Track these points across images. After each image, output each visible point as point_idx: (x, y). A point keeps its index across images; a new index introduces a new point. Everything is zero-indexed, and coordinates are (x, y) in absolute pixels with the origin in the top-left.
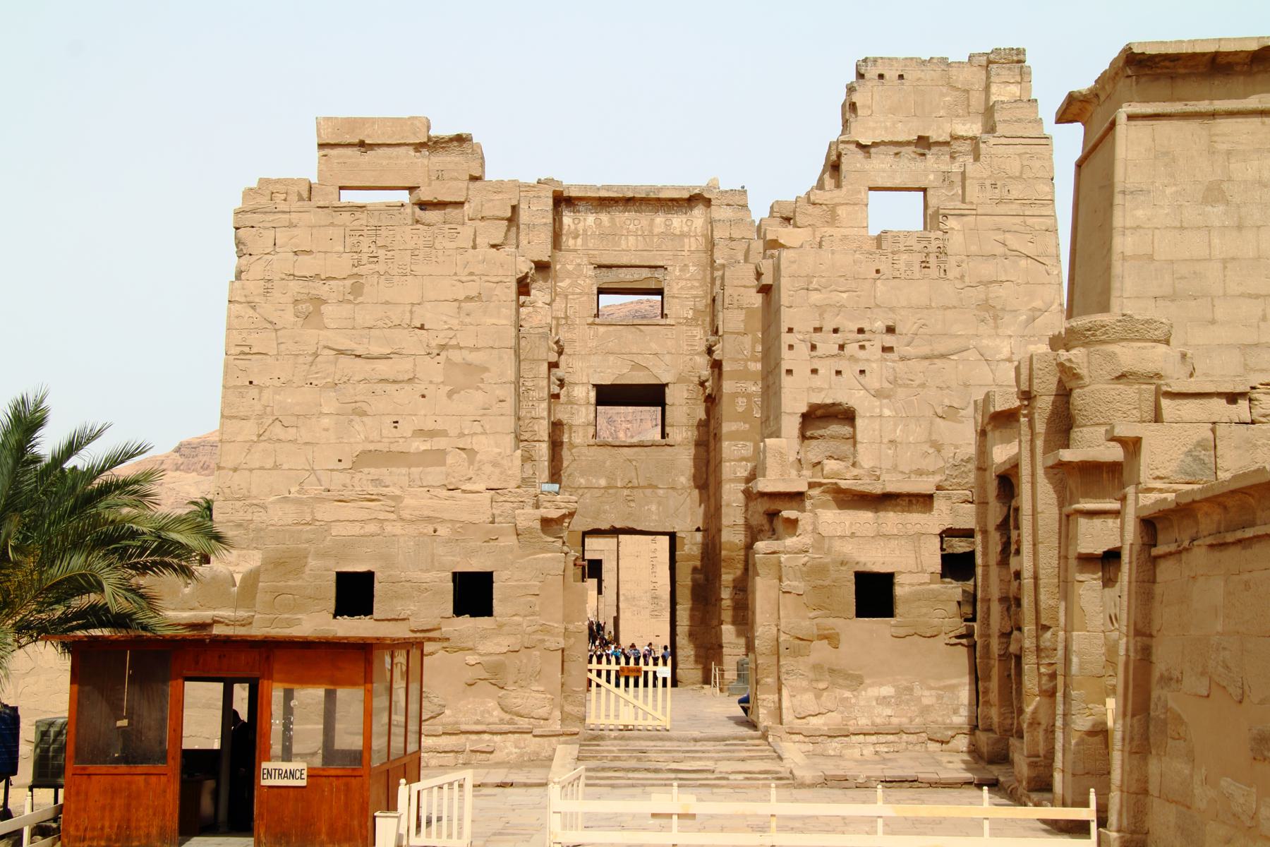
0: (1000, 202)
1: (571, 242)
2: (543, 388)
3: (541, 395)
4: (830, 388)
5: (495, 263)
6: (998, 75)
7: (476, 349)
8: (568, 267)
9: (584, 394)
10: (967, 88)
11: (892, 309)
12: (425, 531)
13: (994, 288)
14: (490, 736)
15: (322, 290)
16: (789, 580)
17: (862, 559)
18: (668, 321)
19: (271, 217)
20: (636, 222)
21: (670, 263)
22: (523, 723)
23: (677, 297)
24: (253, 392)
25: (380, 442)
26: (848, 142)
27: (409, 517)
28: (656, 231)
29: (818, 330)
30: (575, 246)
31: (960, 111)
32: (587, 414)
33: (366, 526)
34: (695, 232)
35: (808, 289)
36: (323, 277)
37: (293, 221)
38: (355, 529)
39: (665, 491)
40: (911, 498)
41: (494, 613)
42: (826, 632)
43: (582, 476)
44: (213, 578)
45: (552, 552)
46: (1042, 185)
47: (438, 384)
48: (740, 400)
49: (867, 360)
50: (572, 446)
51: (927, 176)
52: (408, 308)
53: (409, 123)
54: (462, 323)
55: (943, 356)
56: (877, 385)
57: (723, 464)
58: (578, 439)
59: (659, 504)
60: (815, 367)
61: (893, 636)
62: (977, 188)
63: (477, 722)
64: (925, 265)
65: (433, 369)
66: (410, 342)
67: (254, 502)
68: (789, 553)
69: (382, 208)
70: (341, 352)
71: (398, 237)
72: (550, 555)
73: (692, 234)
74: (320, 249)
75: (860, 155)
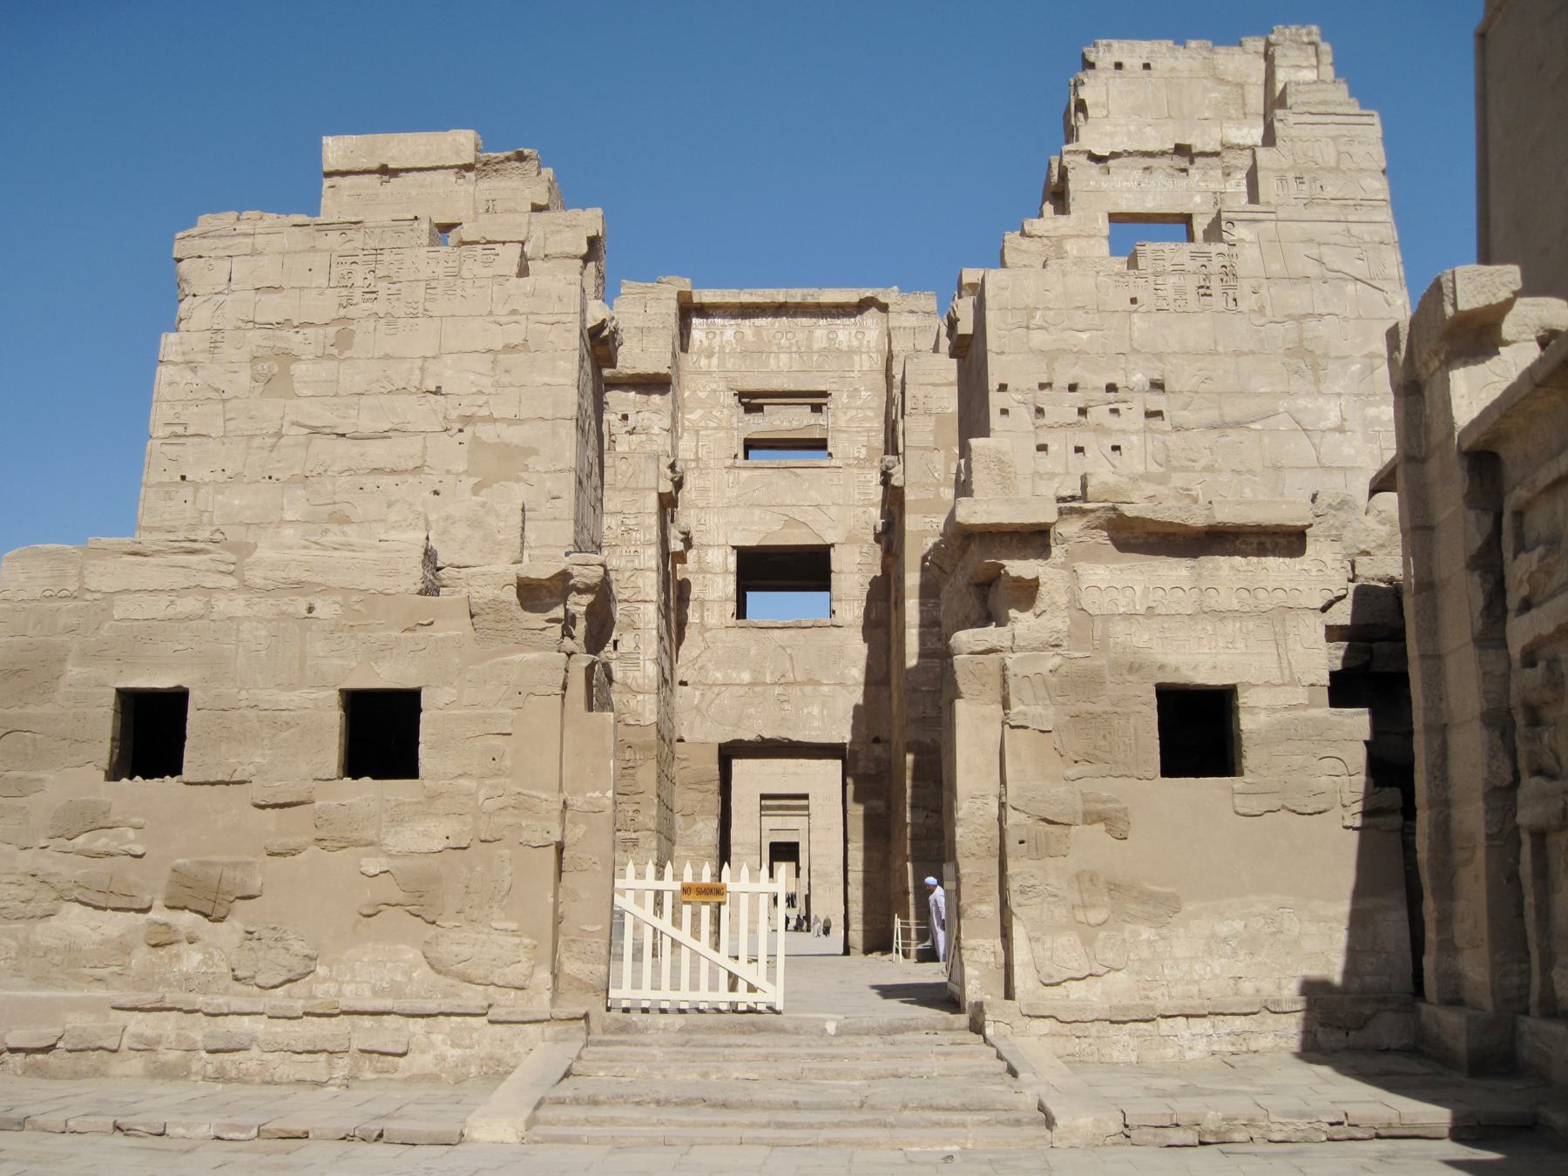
0: (1310, 202)
2: (651, 527)
3: (648, 537)
5: (549, 297)
6: (1285, 56)
7: (516, 421)
8: (700, 394)
9: (721, 559)
10: (1240, 81)
11: (1159, 356)
12: (291, 609)
13: (1313, 323)
14: (402, 1020)
15: (293, 340)
16: (1023, 703)
17: (1171, 659)
18: (834, 462)
19: (228, 242)
20: (789, 335)
21: (834, 387)
22: (473, 997)
23: (844, 431)
24: (186, 492)
26: (1075, 152)
27: (260, 582)
28: (816, 346)
29: (1042, 386)
30: (709, 366)
32: (725, 586)
33: (178, 601)
34: (868, 346)
35: (1028, 328)
36: (295, 323)
37: (256, 246)
38: (158, 607)
39: (831, 687)
40: (1263, 539)
41: (421, 772)
42: (1100, 807)
46: (1369, 179)
47: (458, 474)
49: (1123, 431)
50: (703, 627)
52: (419, 363)
54: (497, 384)
55: (1238, 424)
57: (907, 631)
58: (712, 619)
59: (824, 705)
61: (1237, 813)
62: (1275, 183)
63: (377, 993)
64: (1204, 291)
66: (415, 411)
68: (1022, 649)
70: (315, 431)
72: (532, 656)
73: (863, 350)
74: (292, 284)
75: (1095, 168)
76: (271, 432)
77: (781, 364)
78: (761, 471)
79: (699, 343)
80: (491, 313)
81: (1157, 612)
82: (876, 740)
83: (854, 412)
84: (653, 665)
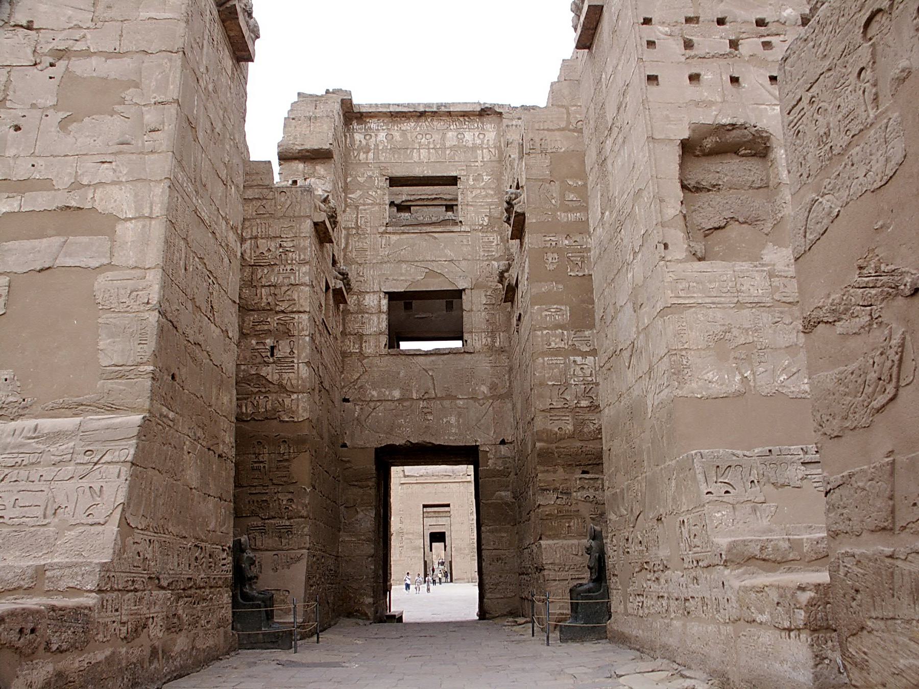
1: (362, 156)
3: (302, 257)
4: (724, 101)
7: (117, 54)
9: (376, 302)
21: (464, 173)
23: (471, 205)
28: (448, 145)
39: (466, 401)
43: (374, 389)
48: (550, 256)
50: (362, 355)
58: (369, 349)
59: (459, 415)
60: (694, 71)
73: (484, 146)
77: (422, 157)
78: (407, 235)
79: (358, 143)
82: (503, 442)
83: (479, 191)
84: (306, 368)
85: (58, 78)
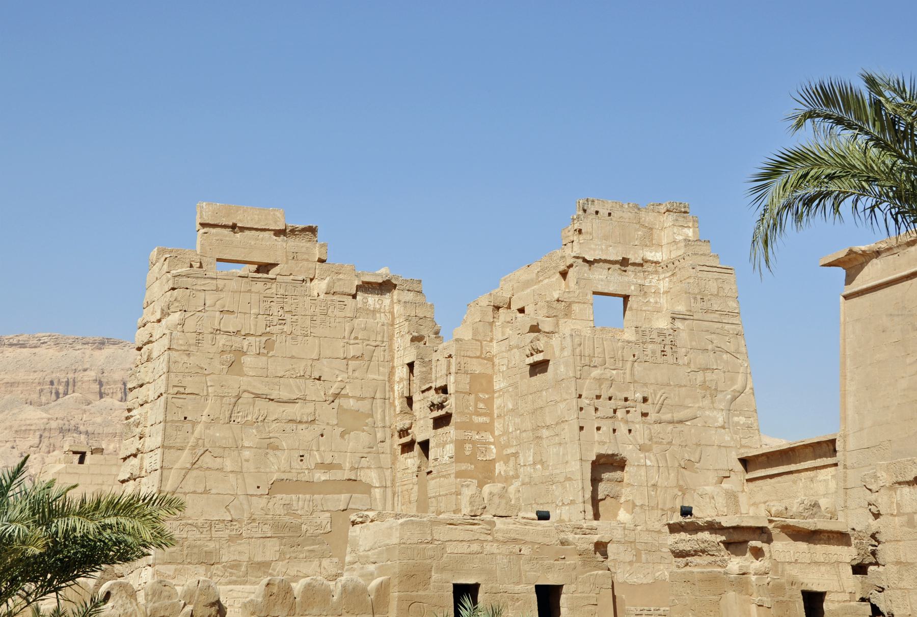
7: (363, 399)
10: (651, 226)
11: (645, 385)
17: (805, 581)
24: (187, 426)
25: (290, 472)
27: (501, 539)
29: (598, 397)
31: (648, 242)
33: (471, 546)
34: (384, 309)
38: (463, 548)
40: (829, 534)
44: (354, 589)
45: (602, 569)
46: (731, 302)
51: (630, 286)
52: (310, 362)
53: (272, 213)
55: (681, 422)
56: (641, 442)
65: (327, 413)
67: (190, 522)
69: (288, 281)
70: (257, 396)
71: (301, 305)
72: (600, 572)
76: (234, 395)
80: (344, 338)
81: (799, 561)
85: (336, 408)
